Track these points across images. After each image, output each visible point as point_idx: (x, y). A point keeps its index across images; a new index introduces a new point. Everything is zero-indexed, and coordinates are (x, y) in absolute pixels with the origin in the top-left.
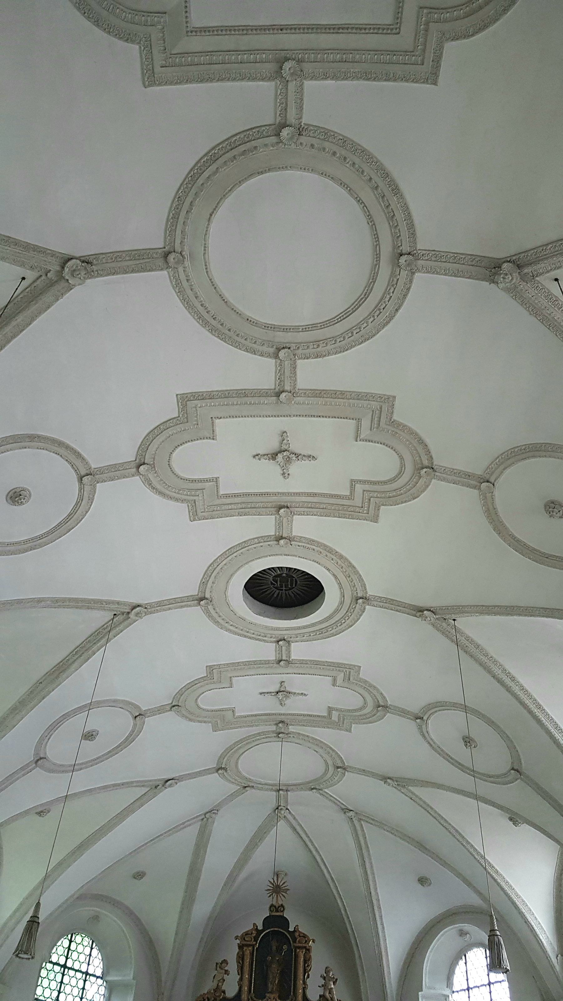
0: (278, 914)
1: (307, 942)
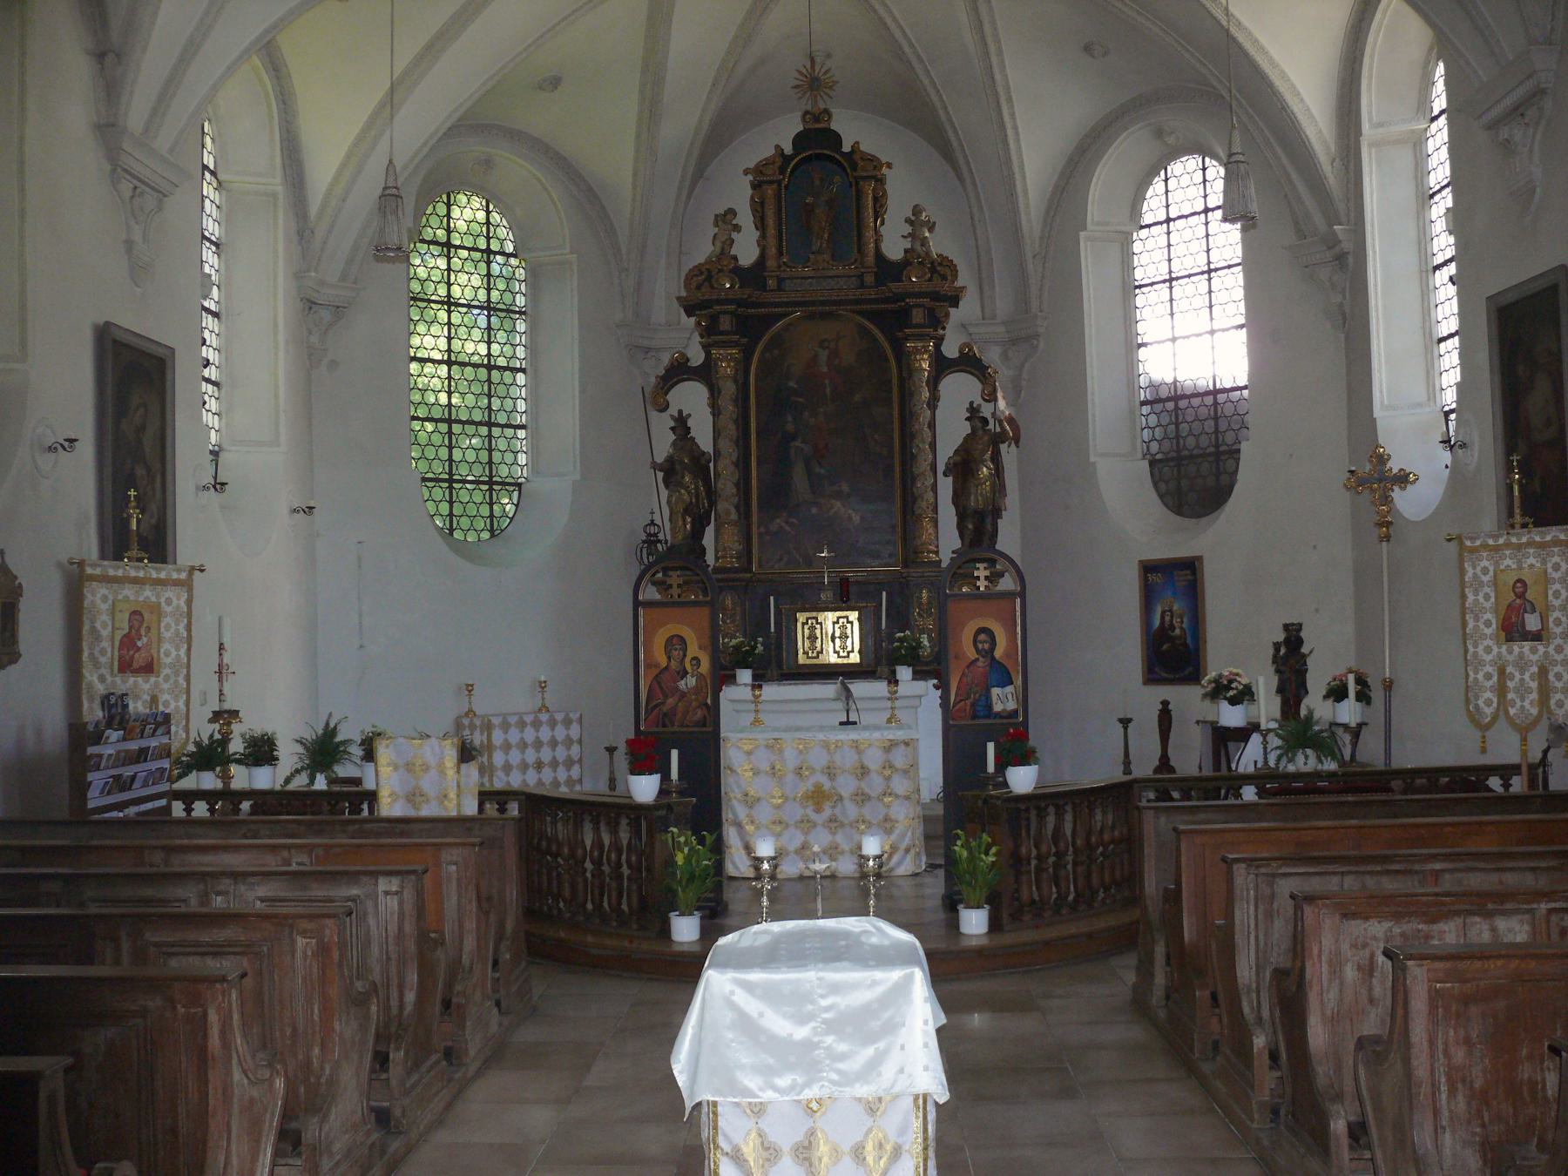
0: (818, 126)
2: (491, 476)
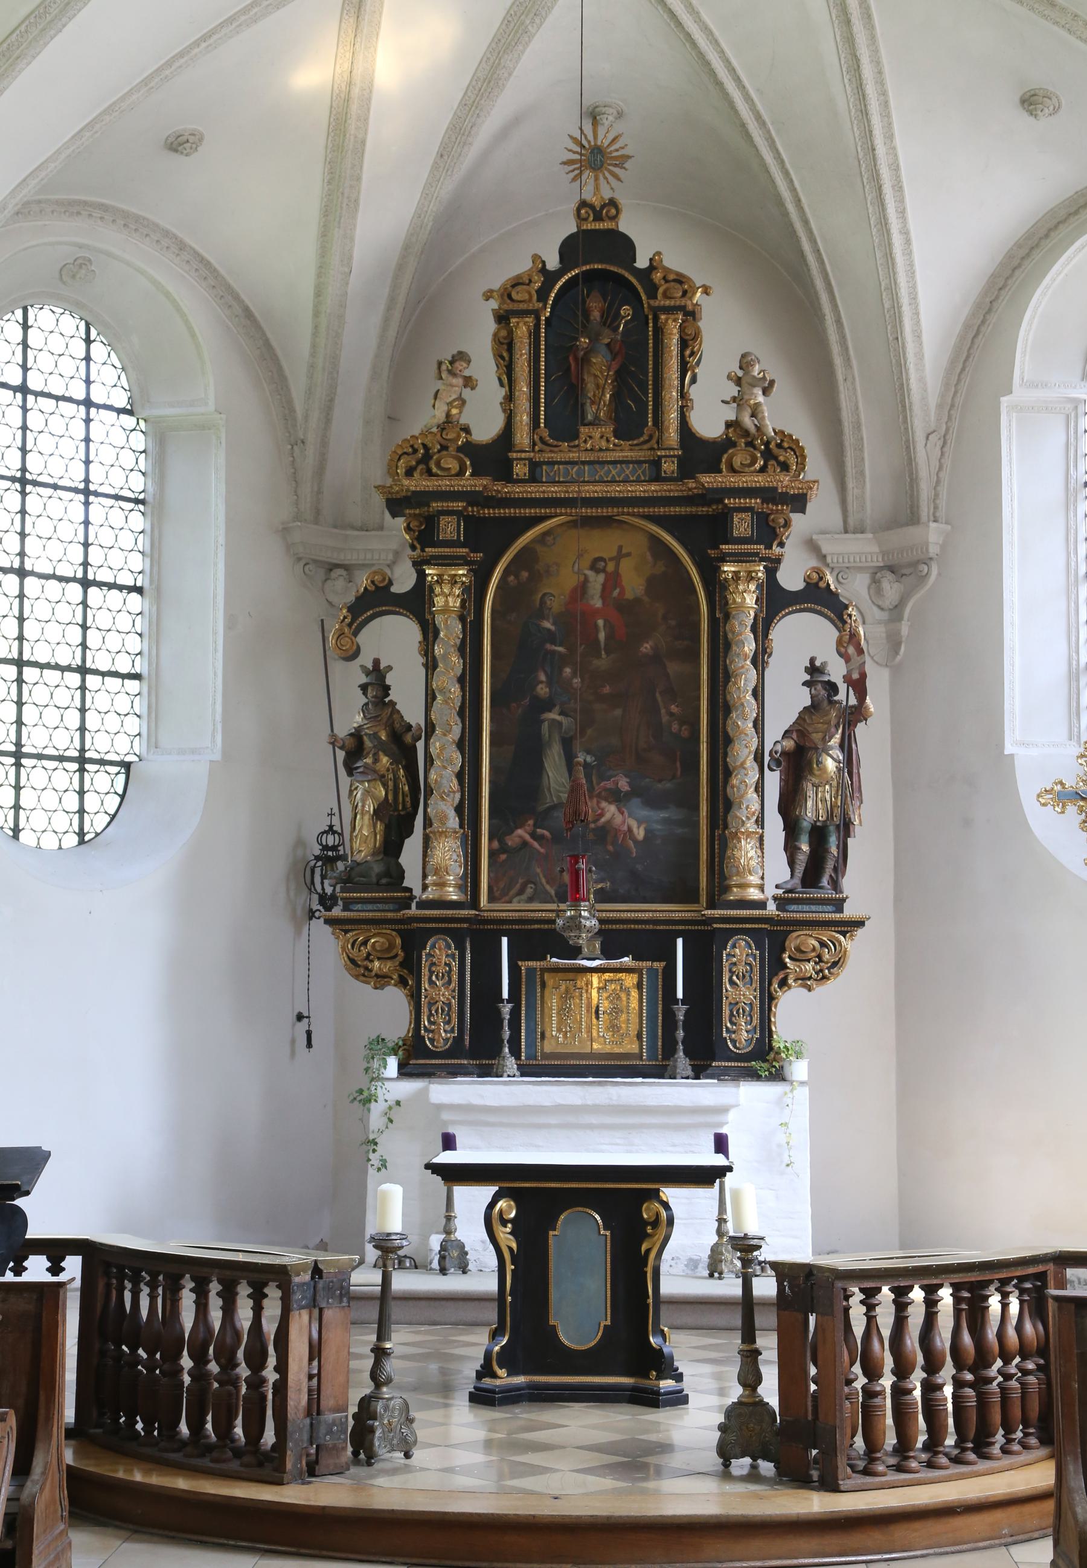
1: (689, 295)
2: (83, 750)
